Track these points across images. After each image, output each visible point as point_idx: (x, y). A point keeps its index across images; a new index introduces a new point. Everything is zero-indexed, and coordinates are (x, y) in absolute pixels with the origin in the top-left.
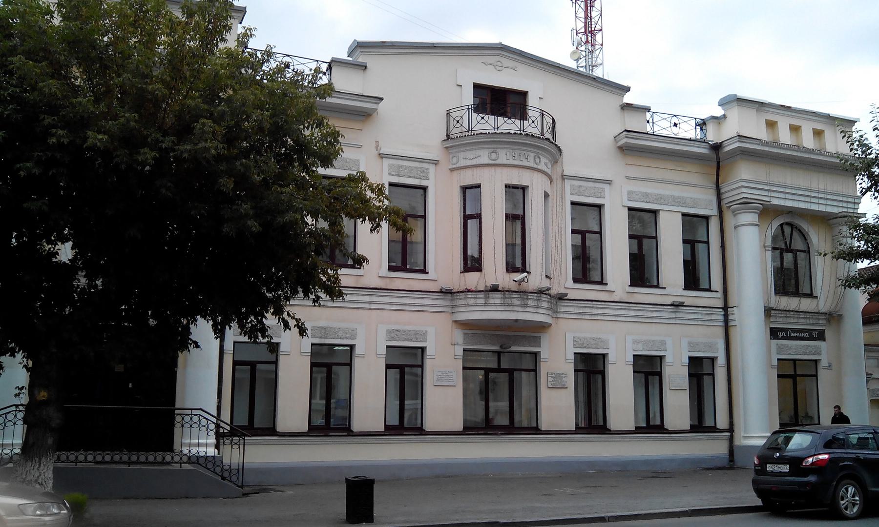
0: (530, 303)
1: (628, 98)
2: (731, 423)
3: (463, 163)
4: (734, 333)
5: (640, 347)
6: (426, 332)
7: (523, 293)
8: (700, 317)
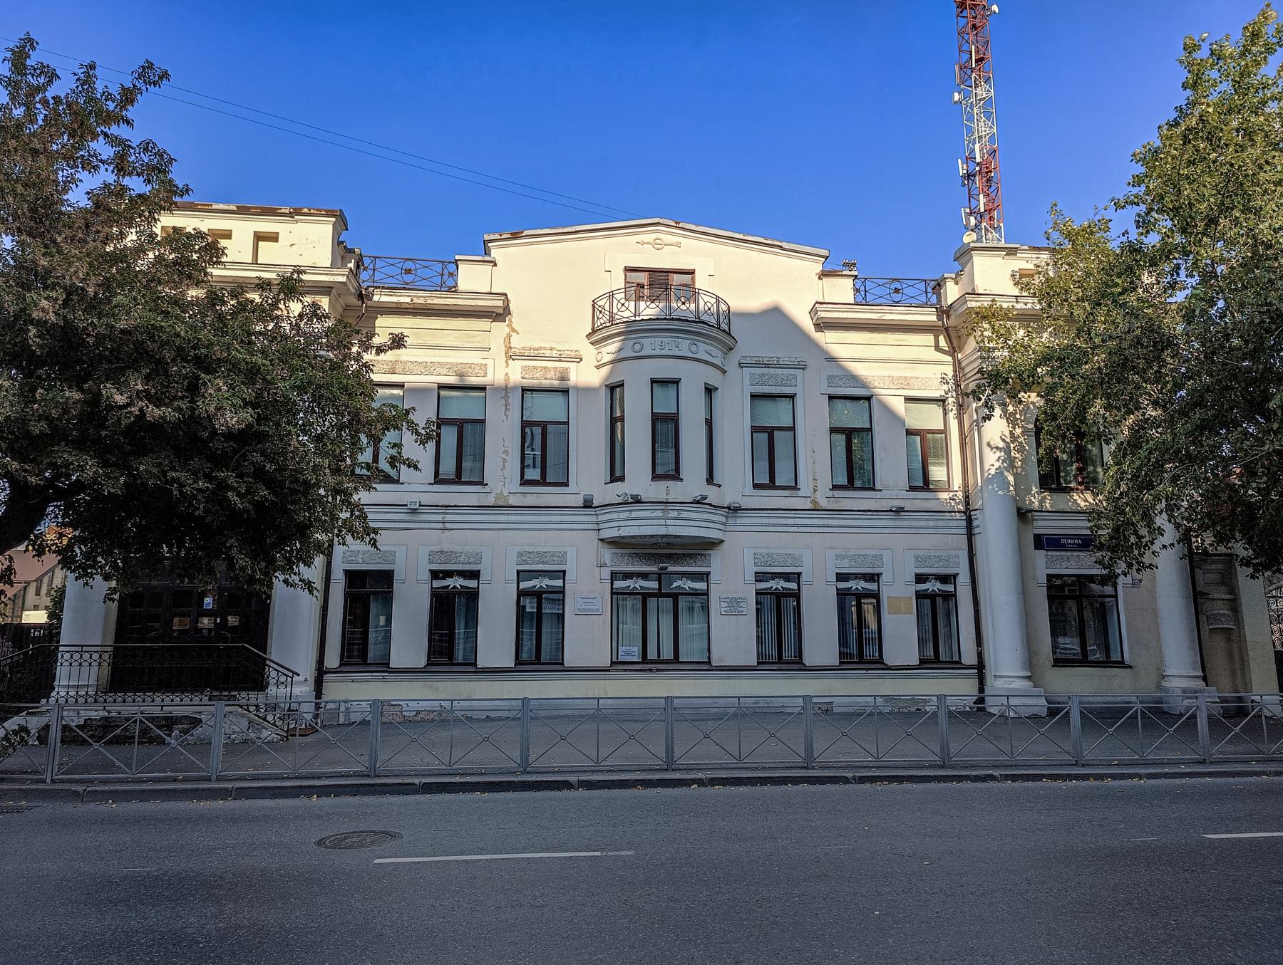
2: (980, 655)
4: (978, 541)
5: (846, 563)
8: (931, 523)
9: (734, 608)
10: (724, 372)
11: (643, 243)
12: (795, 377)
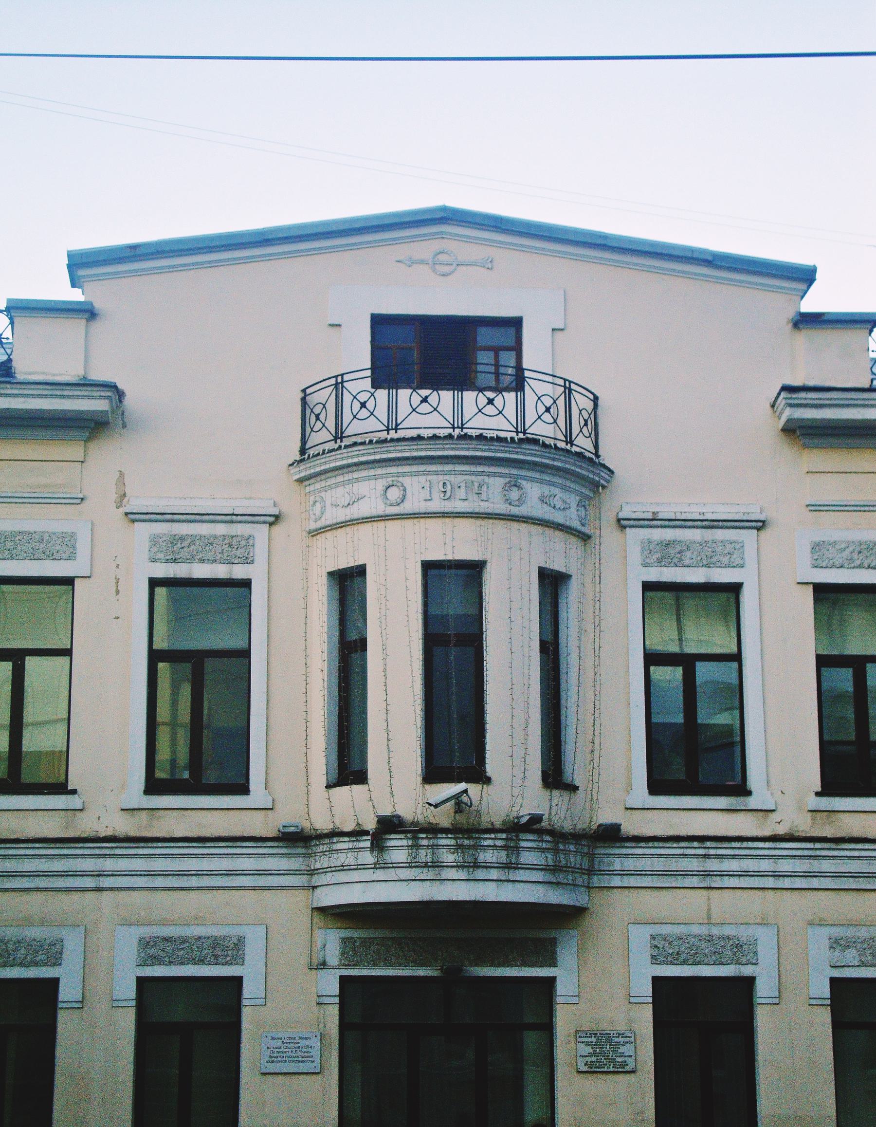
0: (488, 856)
1: (811, 304)
3: (333, 515)
6: (241, 940)
7: (467, 830)
9: (605, 1057)
10: (585, 538)
11: (412, 262)
12: (739, 546)
